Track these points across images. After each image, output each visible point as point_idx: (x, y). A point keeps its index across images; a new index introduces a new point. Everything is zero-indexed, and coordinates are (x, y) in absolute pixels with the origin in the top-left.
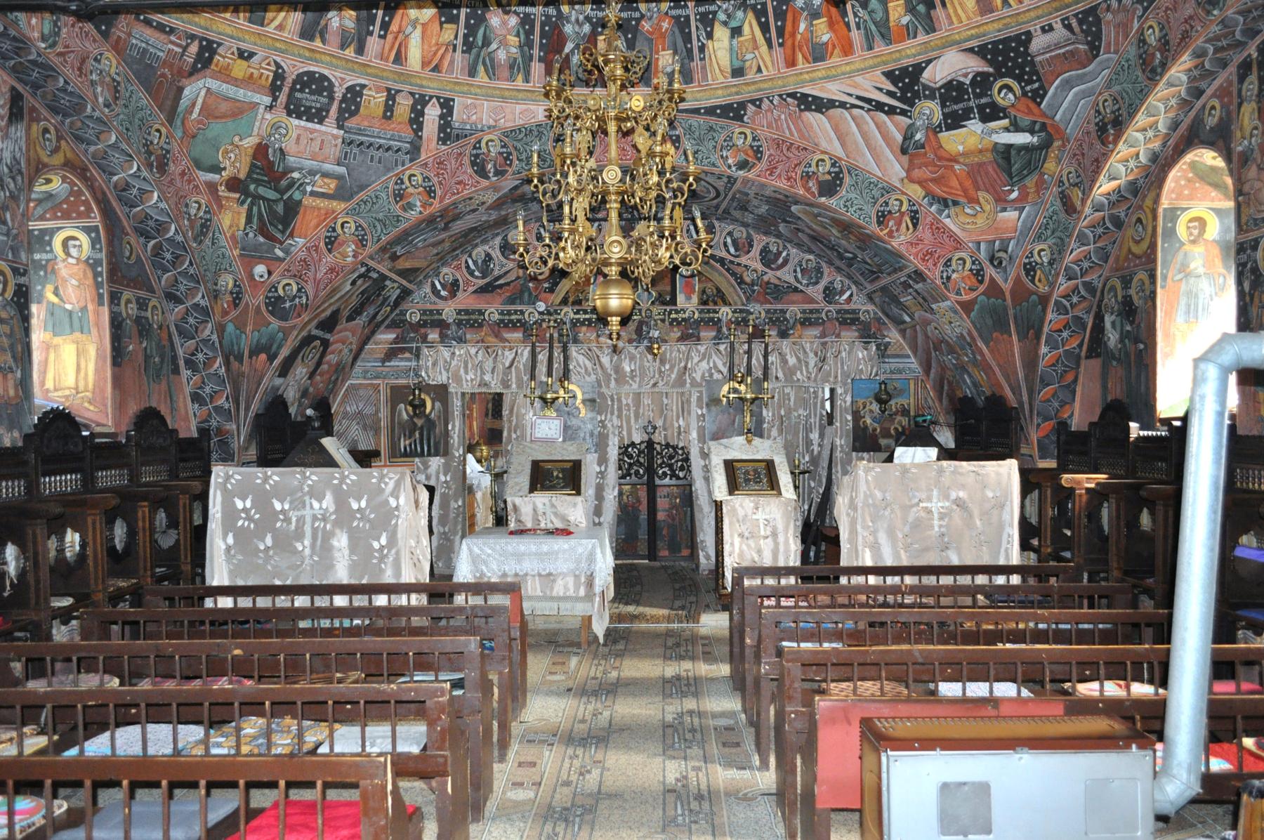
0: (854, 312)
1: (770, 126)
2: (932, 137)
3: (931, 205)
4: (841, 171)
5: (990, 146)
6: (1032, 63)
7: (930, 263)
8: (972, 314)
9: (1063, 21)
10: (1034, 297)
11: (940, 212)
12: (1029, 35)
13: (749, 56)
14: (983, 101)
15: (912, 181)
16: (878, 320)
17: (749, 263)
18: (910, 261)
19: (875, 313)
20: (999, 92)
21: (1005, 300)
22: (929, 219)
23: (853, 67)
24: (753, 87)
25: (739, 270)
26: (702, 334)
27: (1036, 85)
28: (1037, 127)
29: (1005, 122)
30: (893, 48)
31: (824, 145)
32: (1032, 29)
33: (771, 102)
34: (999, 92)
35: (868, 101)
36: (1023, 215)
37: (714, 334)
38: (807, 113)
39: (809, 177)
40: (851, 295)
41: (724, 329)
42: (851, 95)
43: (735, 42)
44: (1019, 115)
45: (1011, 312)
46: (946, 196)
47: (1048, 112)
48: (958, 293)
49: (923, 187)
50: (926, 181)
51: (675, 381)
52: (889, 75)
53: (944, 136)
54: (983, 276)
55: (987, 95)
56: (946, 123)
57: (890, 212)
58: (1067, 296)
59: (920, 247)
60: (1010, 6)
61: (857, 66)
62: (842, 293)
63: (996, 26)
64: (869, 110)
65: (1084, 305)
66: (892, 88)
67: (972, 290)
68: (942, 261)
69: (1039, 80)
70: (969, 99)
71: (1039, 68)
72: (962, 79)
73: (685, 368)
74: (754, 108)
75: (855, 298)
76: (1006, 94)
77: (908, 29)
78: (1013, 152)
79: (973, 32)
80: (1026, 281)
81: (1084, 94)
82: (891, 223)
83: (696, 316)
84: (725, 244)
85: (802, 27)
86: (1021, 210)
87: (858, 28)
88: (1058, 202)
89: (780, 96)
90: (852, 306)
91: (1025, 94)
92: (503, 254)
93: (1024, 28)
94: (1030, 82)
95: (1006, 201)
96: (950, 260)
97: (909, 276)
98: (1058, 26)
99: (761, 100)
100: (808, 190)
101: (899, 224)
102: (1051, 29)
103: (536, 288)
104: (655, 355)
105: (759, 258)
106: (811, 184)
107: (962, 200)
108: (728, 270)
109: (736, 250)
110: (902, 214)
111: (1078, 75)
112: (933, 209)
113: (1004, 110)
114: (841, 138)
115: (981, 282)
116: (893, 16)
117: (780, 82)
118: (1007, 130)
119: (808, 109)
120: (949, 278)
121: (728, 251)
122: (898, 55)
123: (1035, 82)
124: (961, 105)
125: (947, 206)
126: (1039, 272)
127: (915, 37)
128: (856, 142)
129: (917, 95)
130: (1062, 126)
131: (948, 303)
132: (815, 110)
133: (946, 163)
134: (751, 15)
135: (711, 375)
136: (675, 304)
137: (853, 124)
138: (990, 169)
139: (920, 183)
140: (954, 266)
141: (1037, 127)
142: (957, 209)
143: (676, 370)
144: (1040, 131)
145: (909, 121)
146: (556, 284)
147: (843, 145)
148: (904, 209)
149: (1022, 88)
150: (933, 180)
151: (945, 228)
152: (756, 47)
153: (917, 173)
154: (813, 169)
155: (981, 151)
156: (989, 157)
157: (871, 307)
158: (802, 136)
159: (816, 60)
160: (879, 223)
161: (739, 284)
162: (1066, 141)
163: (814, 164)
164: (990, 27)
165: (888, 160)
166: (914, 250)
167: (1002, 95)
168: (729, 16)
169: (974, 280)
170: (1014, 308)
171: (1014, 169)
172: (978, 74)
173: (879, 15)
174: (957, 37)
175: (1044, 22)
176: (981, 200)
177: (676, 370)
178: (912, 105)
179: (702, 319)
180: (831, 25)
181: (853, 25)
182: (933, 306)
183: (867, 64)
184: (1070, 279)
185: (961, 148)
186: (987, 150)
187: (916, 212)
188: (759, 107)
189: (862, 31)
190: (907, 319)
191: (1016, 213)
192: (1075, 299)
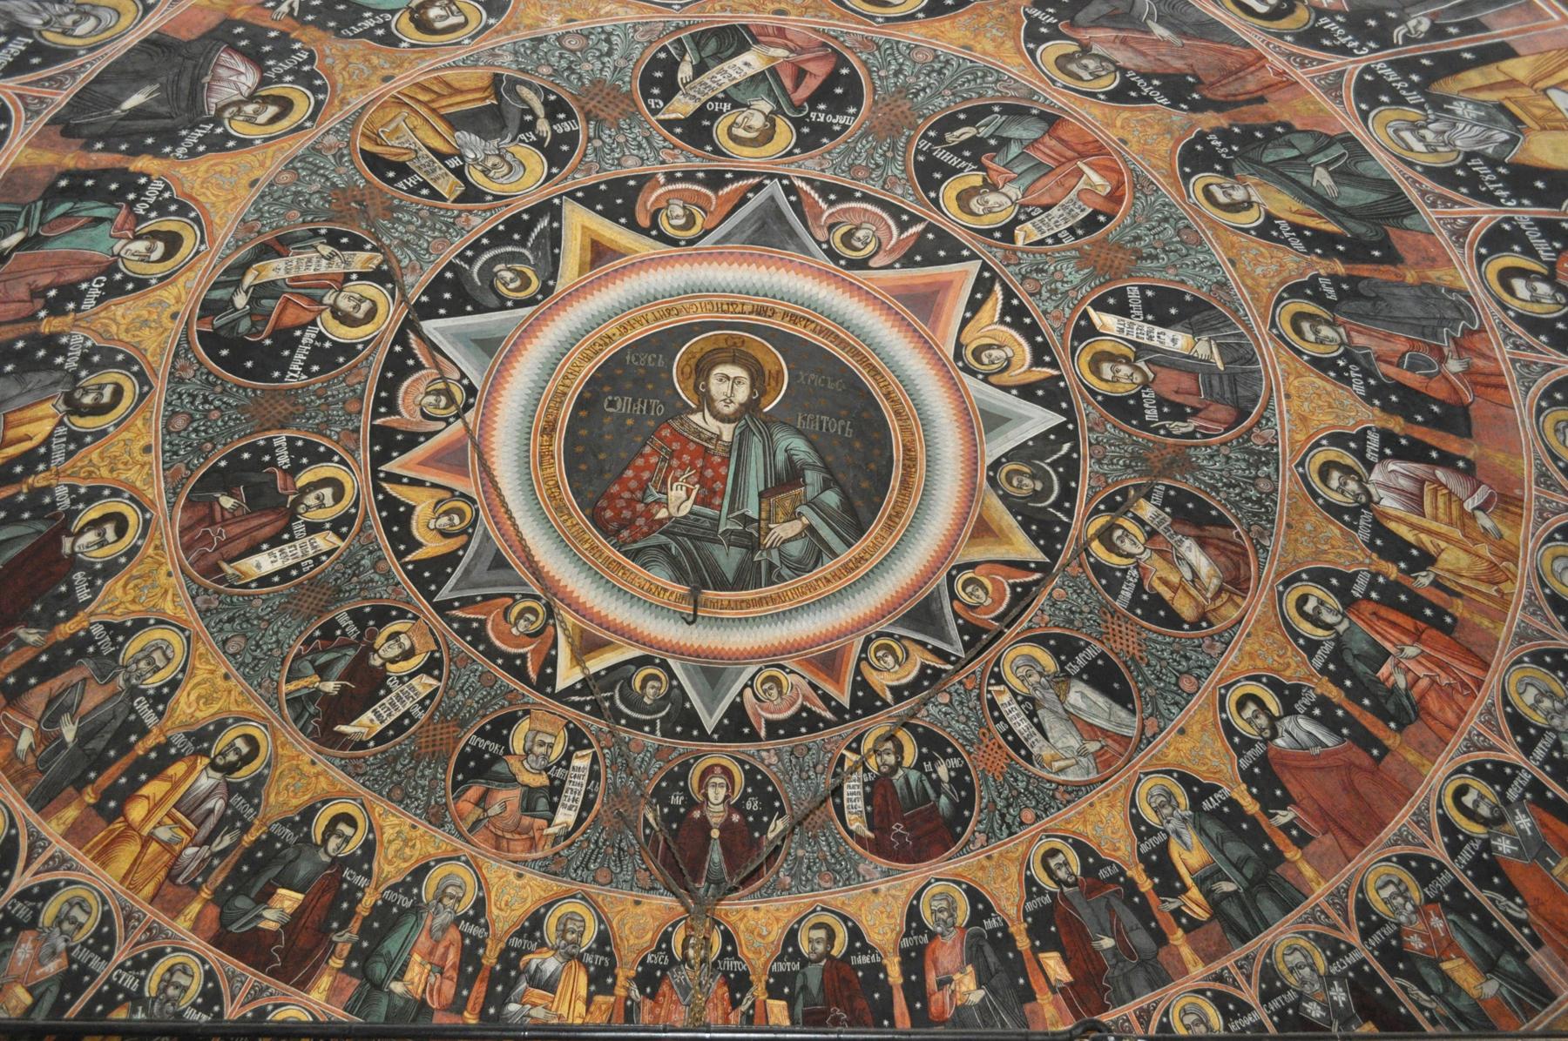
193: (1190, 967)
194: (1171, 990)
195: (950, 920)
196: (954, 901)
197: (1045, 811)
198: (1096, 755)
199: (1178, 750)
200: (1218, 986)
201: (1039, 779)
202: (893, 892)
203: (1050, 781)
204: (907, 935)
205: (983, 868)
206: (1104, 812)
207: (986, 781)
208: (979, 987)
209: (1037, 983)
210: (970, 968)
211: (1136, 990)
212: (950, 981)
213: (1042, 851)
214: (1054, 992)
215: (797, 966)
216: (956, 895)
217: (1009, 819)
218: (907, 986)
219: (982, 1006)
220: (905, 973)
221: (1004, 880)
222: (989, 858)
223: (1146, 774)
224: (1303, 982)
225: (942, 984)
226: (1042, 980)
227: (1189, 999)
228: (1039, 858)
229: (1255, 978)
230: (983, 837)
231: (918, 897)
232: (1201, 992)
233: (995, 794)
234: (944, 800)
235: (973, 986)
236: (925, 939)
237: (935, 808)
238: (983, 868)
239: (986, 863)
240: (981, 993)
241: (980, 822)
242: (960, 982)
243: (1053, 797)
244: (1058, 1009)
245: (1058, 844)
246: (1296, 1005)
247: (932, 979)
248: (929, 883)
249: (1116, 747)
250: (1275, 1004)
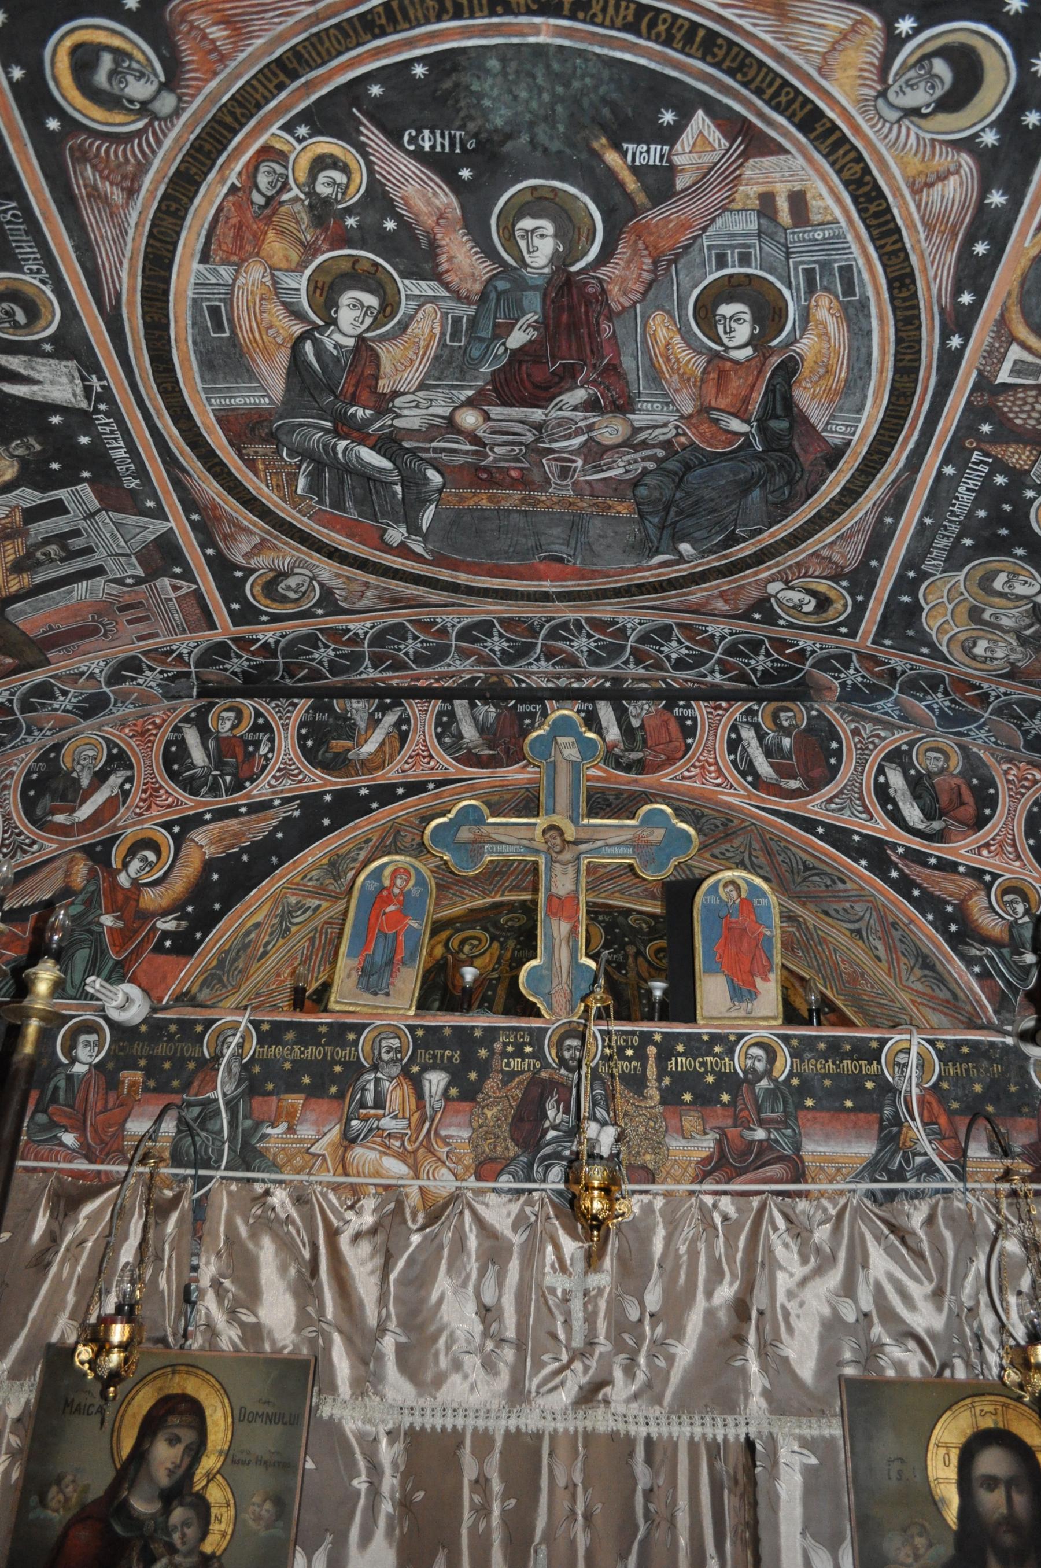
17: (987, 861)
25: (946, 887)
26: (813, 1149)
37: (866, 1149)
41: (916, 1129)
51: (688, 1384)
73: (741, 1308)
83: (783, 1065)
84: (883, 793)
92: (29, 806)
103: (124, 936)
104: (596, 1223)
105: (1024, 845)
108: (904, 886)
109: (929, 815)
121: (897, 817)
135: (872, 1351)
136: (690, 1016)
143: (695, 1322)
146: (207, 921)
161: (956, 941)
177: (695, 1322)
179: (806, 1088)
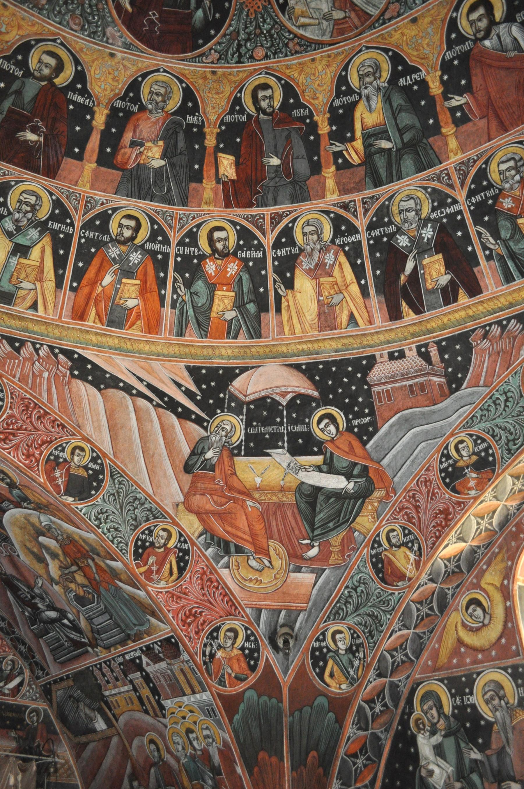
0: (20, 710)
1: (23, 379)
2: (226, 459)
3: (208, 546)
4: (102, 472)
5: (294, 485)
6: (368, 394)
7: (192, 629)
8: (237, 717)
9: (419, 348)
10: (321, 700)
11: (218, 558)
12: (372, 360)
13: (26, 285)
14: (298, 428)
15: (190, 510)
16: (47, 723)
18: (167, 621)
19: (47, 716)
20: (319, 422)
21: (280, 701)
22: (202, 565)
23: (153, 348)
24: (18, 323)
27: (367, 420)
28: (356, 472)
29: (319, 459)
30: (207, 342)
31: (89, 430)
32: (377, 354)
33: (37, 350)
34: (319, 422)
35: (160, 394)
36: (321, 581)
38: (79, 382)
39: (58, 464)
40: (21, 684)
42: (141, 380)
43: (14, 260)
44: (336, 453)
45: (286, 720)
46: (230, 539)
47: (373, 455)
48: (221, 683)
49: (202, 521)
50: (207, 513)
52: (193, 371)
53: (241, 461)
54: (257, 660)
55: (303, 423)
56: (247, 447)
57: (152, 544)
58: (370, 702)
59: (183, 602)
60: (357, 324)
61: (159, 349)
62: (9, 679)
63: (334, 345)
64: (158, 405)
65: (384, 719)
66: (193, 388)
67: (239, 679)
68: (208, 629)
69: (372, 413)
70: (281, 424)
71: (375, 400)
72: (278, 398)
74: (9, 349)
75: (25, 688)
76: (326, 426)
77: (230, 327)
78: (321, 498)
79: (305, 347)
80: (313, 674)
81: (427, 437)
82: (152, 560)
85: (108, 279)
86: (319, 573)
87: (173, 307)
88: (369, 569)
89: (52, 348)
90: (19, 701)
91: (350, 429)
93: (369, 352)
94: (357, 416)
95: (302, 558)
96: (217, 629)
97: (148, 650)
98: (411, 354)
99: (23, 343)
100: (52, 479)
101: (161, 563)
102: (402, 355)
106: (57, 474)
107: (248, 547)
110: (168, 551)
111: (423, 414)
112: (210, 552)
113: (320, 443)
114: (112, 429)
115: (253, 669)
116: (218, 306)
117: (56, 331)
118: (319, 469)
119: (83, 377)
120: (212, 656)
122: (210, 351)
123: (366, 416)
124: (270, 429)
125: (227, 552)
126: (330, 663)
127: (236, 337)
128: (130, 440)
129: (220, 404)
130: (389, 473)
131: (206, 696)
132: (91, 383)
133: (236, 495)
134: (47, 241)
137: (133, 416)
138: (289, 513)
139: (199, 514)
140: (221, 640)
141: (356, 472)
142: (241, 558)
144: (359, 476)
145: (203, 433)
147: (114, 438)
148: (171, 544)
149: (348, 421)
150: (214, 513)
151: (220, 581)
152: (40, 277)
153: (197, 500)
154: (64, 455)
155: (282, 489)
156: (289, 498)
157: (42, 706)
158: (63, 408)
159: (111, 323)
160: (137, 555)
162: (392, 490)
163: (68, 449)
164: (327, 346)
165: (165, 475)
166: (175, 606)
167: (322, 426)
168: (18, 229)
169: (244, 665)
170: (292, 714)
171: (316, 519)
172: (299, 396)
173: (201, 301)
174: (284, 349)
175: (395, 347)
176: (272, 552)
178: (212, 414)
180: (143, 291)
181: (168, 300)
182: (168, 703)
183: (171, 350)
184: (380, 675)
185: (258, 480)
186: (289, 489)
187: (186, 552)
188: (18, 350)
189: (177, 312)
190: (100, 725)
191: (313, 576)
192: (378, 708)
193: (328, 194)
194: (305, 206)
195: (161, 104)
196: (171, 92)
197: (275, 53)
198: (337, 22)
199: (403, 34)
200: (342, 212)
201: (283, 27)
202: (126, 63)
203: (290, 32)
204: (123, 99)
205: (205, 78)
206: (320, 68)
207: (241, 13)
208: (162, 158)
209: (208, 172)
210: (161, 143)
211: (279, 198)
212: (142, 145)
213: (257, 83)
214: (218, 182)
215: (20, 73)
216: (175, 89)
217: (243, 50)
218: (105, 134)
219: (158, 171)
220: (108, 124)
221: (217, 93)
222: (214, 73)
223: (368, 48)
224: (405, 221)
225: (133, 144)
226: (213, 171)
227: (315, 216)
228: (252, 87)
229: (371, 213)
230: (217, 56)
231: (144, 76)
232: (327, 213)
233: (242, 26)
234: (200, 13)
235: (158, 155)
236: (136, 109)
237: (190, 16)
238: (205, 78)
239: (209, 76)
240: (162, 163)
241: (220, 43)
242: (150, 149)
243: (287, 45)
244: (216, 193)
245: (272, 81)
246: (391, 236)
247: (128, 137)
248: (158, 71)
249: (356, 20)
250: (376, 233)
